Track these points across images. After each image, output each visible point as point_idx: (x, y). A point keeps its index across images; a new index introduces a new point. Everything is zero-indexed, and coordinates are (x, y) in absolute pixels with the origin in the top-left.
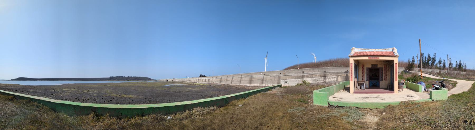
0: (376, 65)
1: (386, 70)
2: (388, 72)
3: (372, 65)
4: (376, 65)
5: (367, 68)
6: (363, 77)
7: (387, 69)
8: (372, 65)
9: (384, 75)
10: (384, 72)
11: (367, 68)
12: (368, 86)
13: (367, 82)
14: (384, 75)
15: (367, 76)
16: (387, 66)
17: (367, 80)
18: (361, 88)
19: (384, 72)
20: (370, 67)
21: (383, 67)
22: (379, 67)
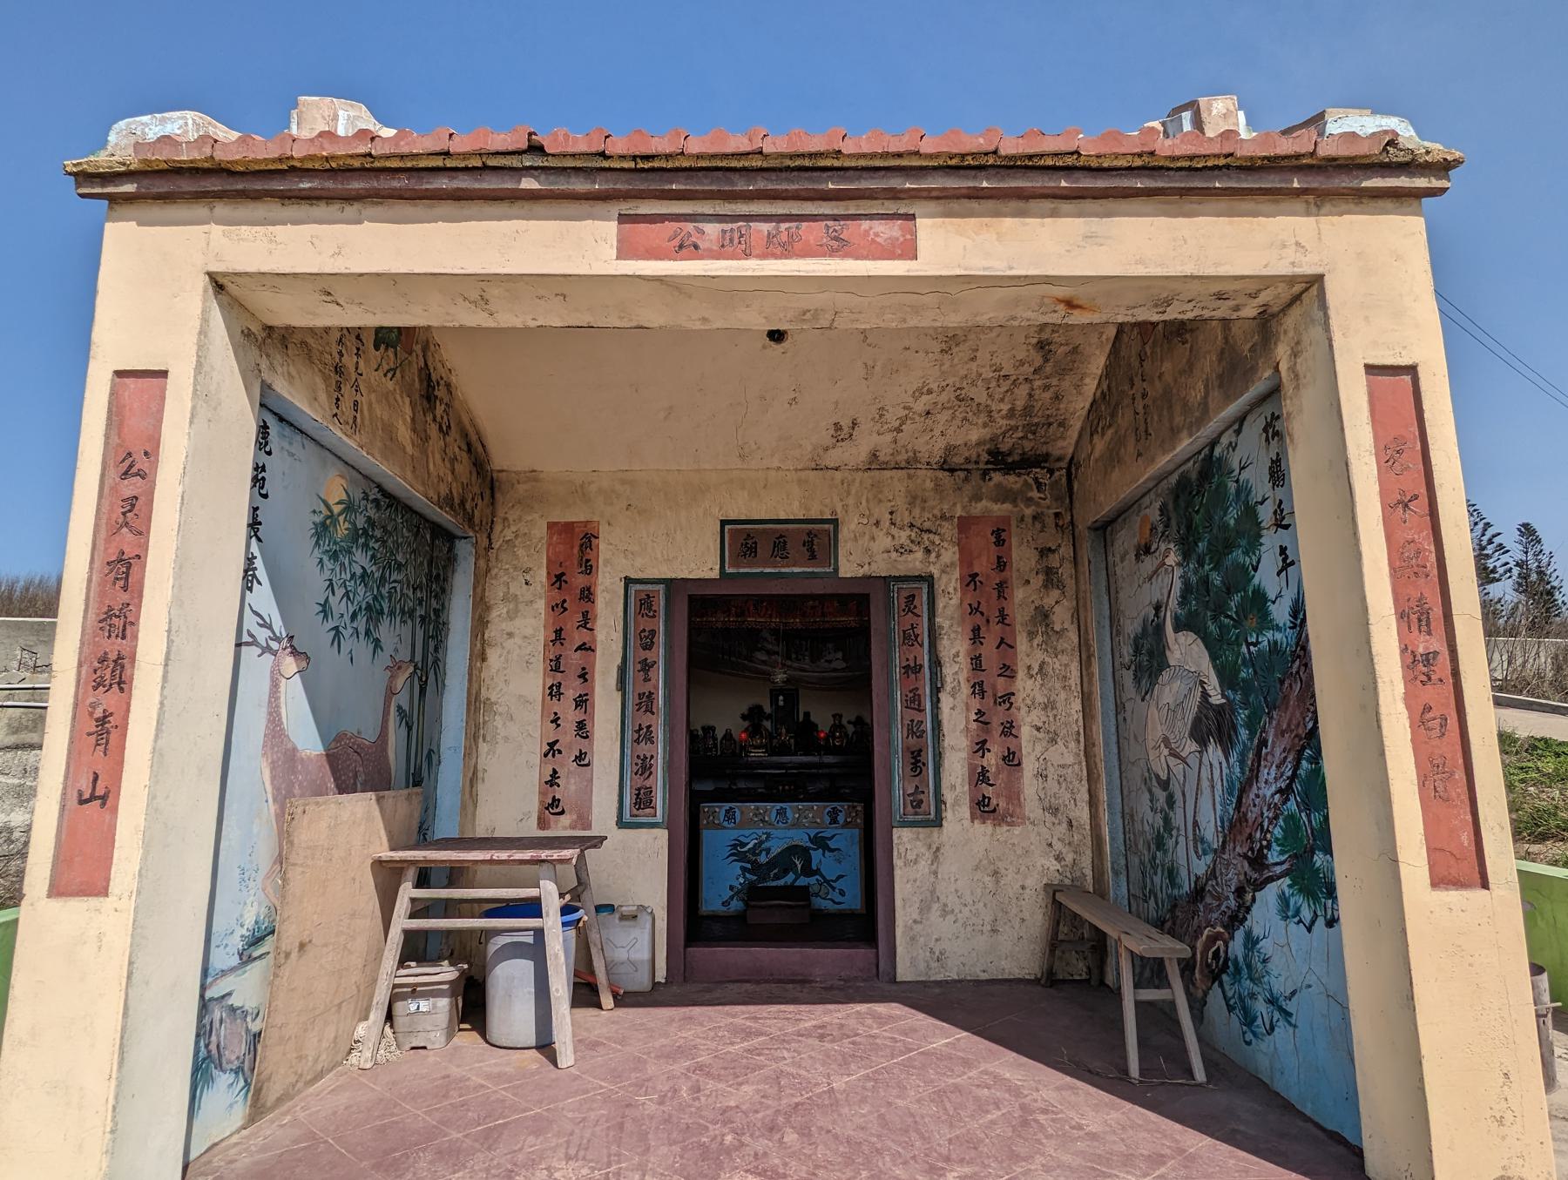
0: (817, 538)
1: (989, 617)
2: (1027, 652)
3: (743, 538)
4: (817, 538)
5: (641, 596)
6: (564, 751)
7: (1022, 598)
8: (743, 538)
9: (956, 715)
10: (955, 649)
11: (641, 596)
12: (640, 947)
13: (638, 868)
14: (956, 715)
15: (636, 735)
16: (1022, 556)
17: (636, 808)
18: (472, 1006)
19: (955, 649)
20: (697, 559)
21: (945, 568)
22: (861, 555)
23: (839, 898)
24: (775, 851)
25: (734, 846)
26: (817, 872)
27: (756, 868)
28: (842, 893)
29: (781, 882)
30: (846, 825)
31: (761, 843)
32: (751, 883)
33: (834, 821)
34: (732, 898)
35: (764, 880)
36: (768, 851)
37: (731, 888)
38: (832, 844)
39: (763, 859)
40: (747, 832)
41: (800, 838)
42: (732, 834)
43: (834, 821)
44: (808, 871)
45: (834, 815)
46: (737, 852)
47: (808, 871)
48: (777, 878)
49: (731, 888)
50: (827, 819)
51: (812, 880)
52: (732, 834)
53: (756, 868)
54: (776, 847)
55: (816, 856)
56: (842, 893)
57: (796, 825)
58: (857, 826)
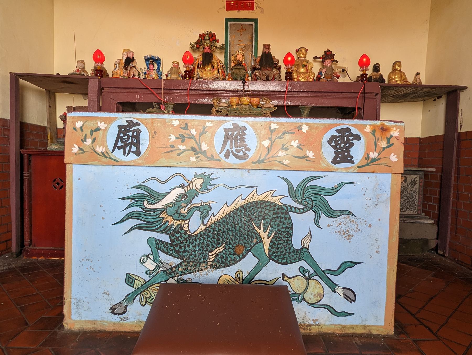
23: (340, 304)
24: (219, 211)
25: (136, 199)
26: (303, 254)
27: (179, 242)
28: (350, 295)
29: (227, 274)
30: (369, 164)
31: (193, 194)
32: (170, 272)
33: (343, 156)
34: (130, 298)
35: (197, 266)
36: (205, 210)
37: (130, 280)
38: (334, 202)
39: (195, 225)
40: (163, 174)
41: (271, 187)
42: (128, 175)
43: (343, 156)
44: (283, 250)
45: (342, 149)
46: (143, 210)
47: (283, 250)
48: (221, 263)
49: (130, 280)
50: (329, 153)
51: (292, 269)
52: (128, 175)
53: (179, 242)
54: (222, 201)
55: (302, 223)
56: (350, 295)
57: (264, 164)
58: (388, 168)
